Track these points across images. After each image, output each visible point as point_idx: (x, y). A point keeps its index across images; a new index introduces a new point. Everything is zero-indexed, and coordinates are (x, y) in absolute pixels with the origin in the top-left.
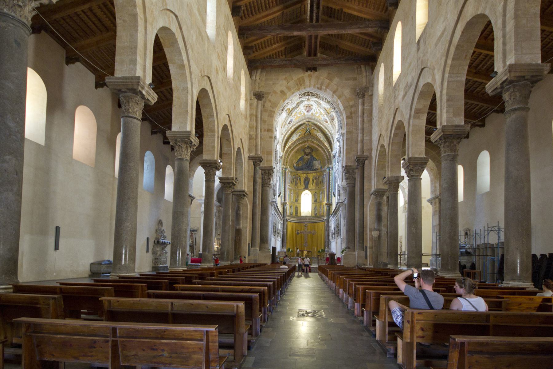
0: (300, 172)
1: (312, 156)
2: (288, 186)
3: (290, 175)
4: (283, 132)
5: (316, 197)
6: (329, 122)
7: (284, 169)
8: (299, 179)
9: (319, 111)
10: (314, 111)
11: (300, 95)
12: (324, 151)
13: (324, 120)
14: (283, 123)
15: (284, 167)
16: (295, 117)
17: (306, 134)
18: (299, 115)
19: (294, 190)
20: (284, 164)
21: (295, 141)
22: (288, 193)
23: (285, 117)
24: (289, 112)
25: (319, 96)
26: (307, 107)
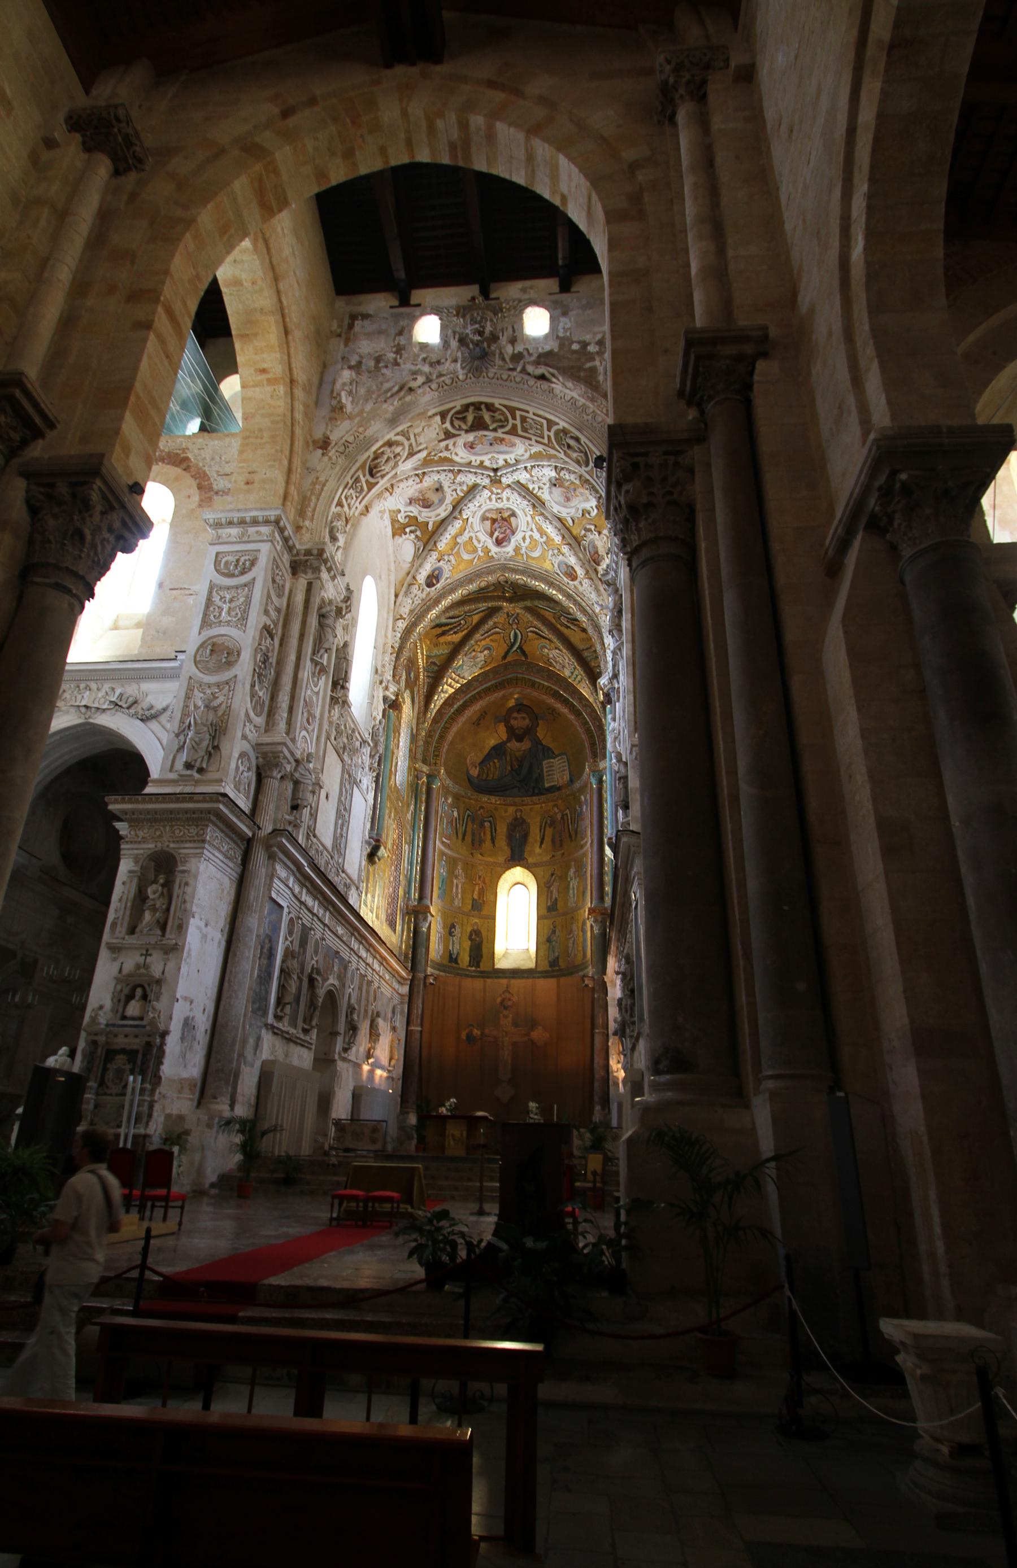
0: (493, 799)
1: (538, 742)
2: (438, 844)
3: (452, 806)
4: (405, 611)
5: (555, 895)
6: (580, 572)
7: (425, 779)
8: (487, 824)
9: (542, 532)
10: (524, 539)
11: (443, 415)
12: (578, 714)
13: (564, 568)
14: (404, 579)
15: (425, 769)
16: (453, 562)
17: (508, 659)
18: (466, 557)
19: (468, 867)
20: (424, 762)
21: (469, 682)
22: (438, 871)
23: (410, 559)
24: (427, 537)
25: (524, 419)
26: (494, 521)
